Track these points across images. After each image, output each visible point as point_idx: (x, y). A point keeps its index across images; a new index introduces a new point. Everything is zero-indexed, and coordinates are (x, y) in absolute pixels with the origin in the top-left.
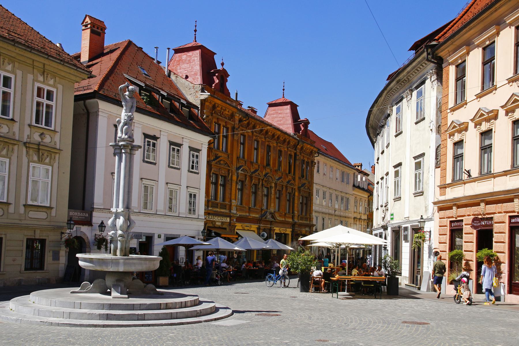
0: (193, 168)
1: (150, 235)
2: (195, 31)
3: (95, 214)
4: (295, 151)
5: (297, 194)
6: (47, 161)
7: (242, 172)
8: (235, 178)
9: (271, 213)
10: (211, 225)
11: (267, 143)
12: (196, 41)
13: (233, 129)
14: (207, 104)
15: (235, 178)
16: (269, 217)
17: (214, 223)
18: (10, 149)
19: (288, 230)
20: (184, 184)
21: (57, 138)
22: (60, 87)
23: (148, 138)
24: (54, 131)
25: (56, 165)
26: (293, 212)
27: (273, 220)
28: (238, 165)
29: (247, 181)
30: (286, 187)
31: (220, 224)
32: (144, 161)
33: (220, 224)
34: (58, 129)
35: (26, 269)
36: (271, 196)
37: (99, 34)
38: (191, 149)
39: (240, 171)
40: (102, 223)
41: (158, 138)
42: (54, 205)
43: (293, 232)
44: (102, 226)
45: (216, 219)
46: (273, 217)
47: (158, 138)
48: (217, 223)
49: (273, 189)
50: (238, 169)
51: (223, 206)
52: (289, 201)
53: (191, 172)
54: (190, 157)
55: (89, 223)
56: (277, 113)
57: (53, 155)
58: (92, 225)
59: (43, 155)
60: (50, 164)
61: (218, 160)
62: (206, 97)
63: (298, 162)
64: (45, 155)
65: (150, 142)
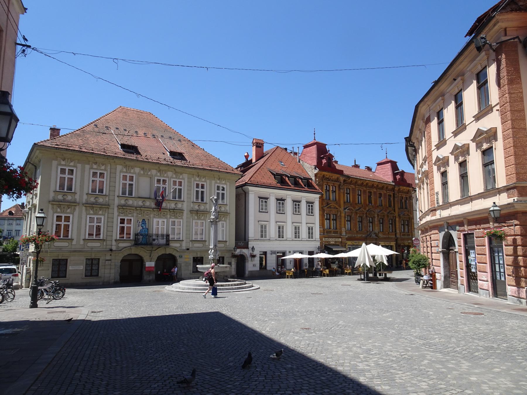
0: (310, 212)
1: (284, 252)
2: (314, 134)
3: (249, 243)
4: (393, 192)
5: (397, 219)
6: (223, 219)
7: (348, 211)
8: (343, 215)
9: (375, 233)
10: (327, 244)
11: (368, 191)
12: (315, 140)
13: (339, 186)
14: (318, 175)
15: (343, 215)
16: (373, 236)
17: (329, 242)
18: (205, 216)
19: (392, 243)
20: (304, 222)
21: (228, 208)
22: (228, 184)
23: (279, 200)
24: (226, 205)
25: (228, 221)
26: (396, 231)
27: (377, 237)
28: (345, 207)
29: (353, 215)
30: (388, 216)
31: (334, 242)
32: (277, 213)
33: (334, 242)
34: (228, 203)
35: (193, 272)
36: (375, 223)
37: (260, 147)
38: (308, 202)
39: (346, 210)
40: (253, 247)
41: (285, 200)
42: (228, 240)
43: (396, 244)
44: (253, 248)
45: (330, 239)
46: (376, 236)
47: (285, 200)
48: (331, 242)
49: (376, 218)
50: (345, 209)
51: (336, 233)
52: (392, 224)
53: (309, 215)
54: (307, 207)
55: (247, 248)
56: (382, 169)
57: (226, 216)
58: (248, 248)
59: (221, 217)
60: (225, 221)
61: (328, 206)
62: (317, 172)
63: (396, 199)
64: (222, 217)
65: (280, 202)
